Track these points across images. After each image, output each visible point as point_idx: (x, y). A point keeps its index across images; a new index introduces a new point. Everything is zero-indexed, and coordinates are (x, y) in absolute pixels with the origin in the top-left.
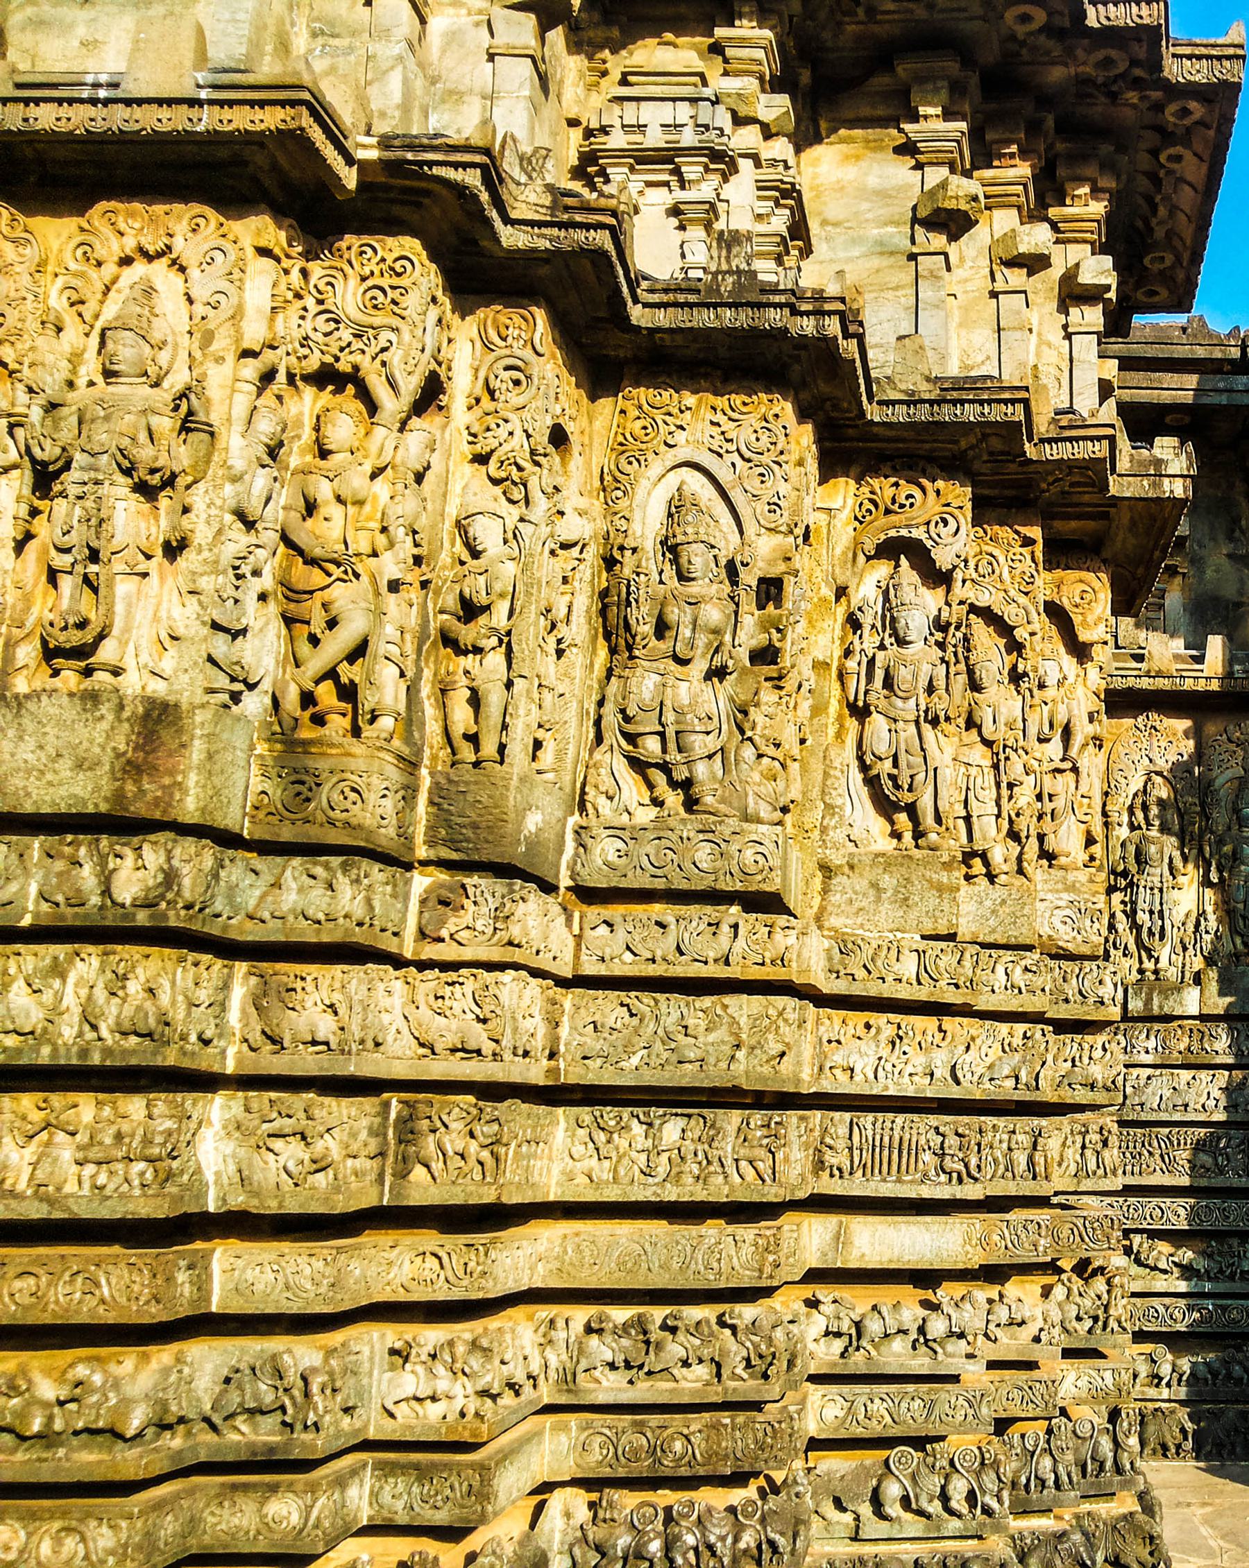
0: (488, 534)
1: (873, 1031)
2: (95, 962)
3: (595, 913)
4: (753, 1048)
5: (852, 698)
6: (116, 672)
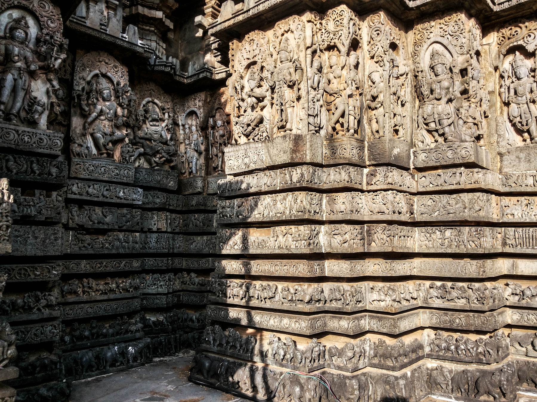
0: (376, 77)
1: (520, 202)
2: (291, 196)
3: (420, 174)
4: (471, 208)
5: (504, 100)
6: (291, 130)
